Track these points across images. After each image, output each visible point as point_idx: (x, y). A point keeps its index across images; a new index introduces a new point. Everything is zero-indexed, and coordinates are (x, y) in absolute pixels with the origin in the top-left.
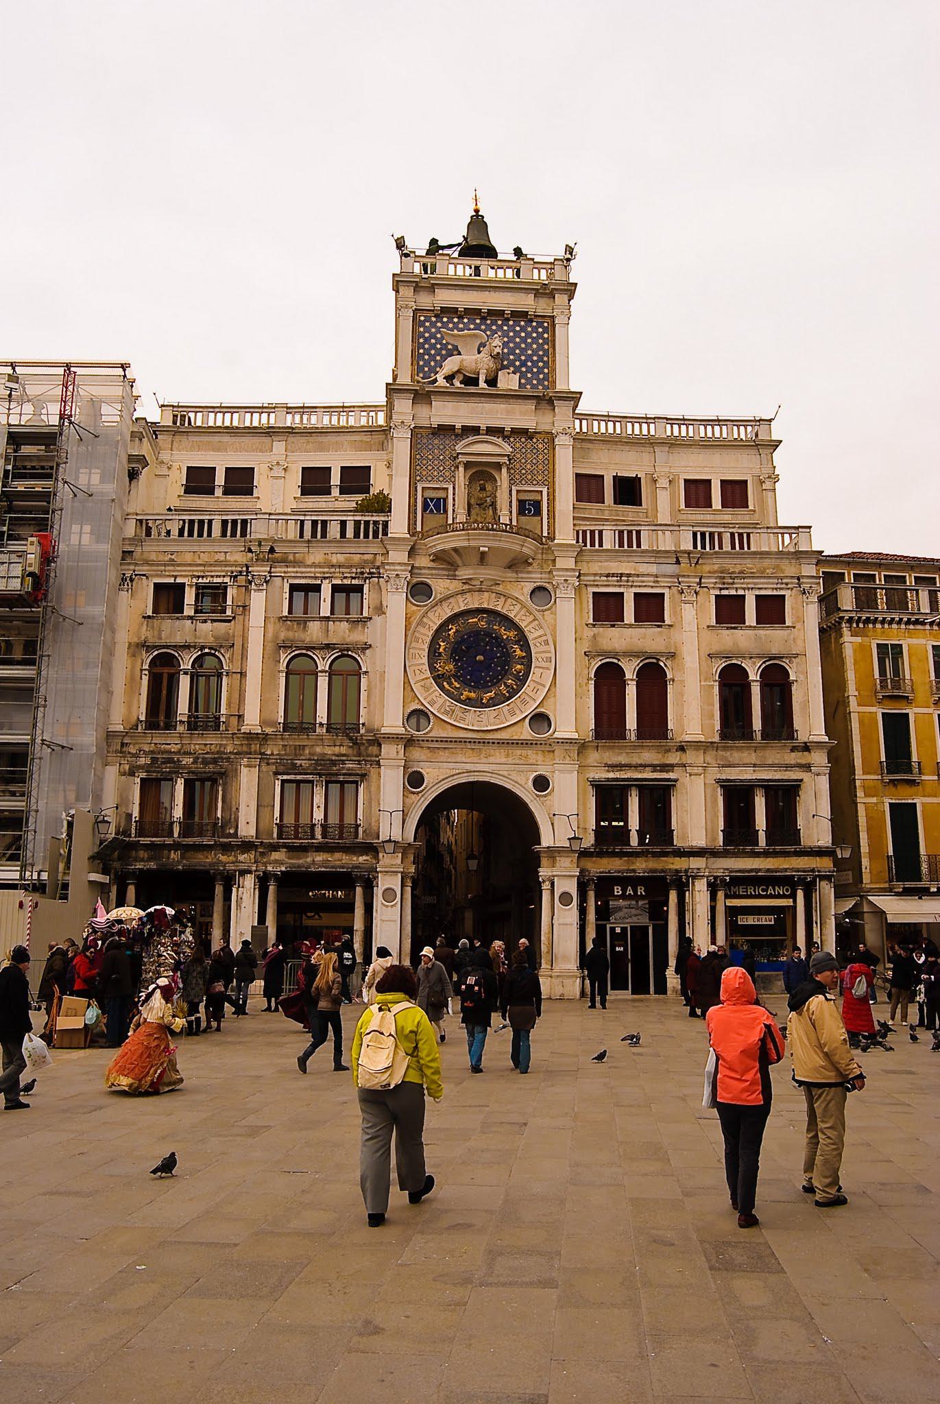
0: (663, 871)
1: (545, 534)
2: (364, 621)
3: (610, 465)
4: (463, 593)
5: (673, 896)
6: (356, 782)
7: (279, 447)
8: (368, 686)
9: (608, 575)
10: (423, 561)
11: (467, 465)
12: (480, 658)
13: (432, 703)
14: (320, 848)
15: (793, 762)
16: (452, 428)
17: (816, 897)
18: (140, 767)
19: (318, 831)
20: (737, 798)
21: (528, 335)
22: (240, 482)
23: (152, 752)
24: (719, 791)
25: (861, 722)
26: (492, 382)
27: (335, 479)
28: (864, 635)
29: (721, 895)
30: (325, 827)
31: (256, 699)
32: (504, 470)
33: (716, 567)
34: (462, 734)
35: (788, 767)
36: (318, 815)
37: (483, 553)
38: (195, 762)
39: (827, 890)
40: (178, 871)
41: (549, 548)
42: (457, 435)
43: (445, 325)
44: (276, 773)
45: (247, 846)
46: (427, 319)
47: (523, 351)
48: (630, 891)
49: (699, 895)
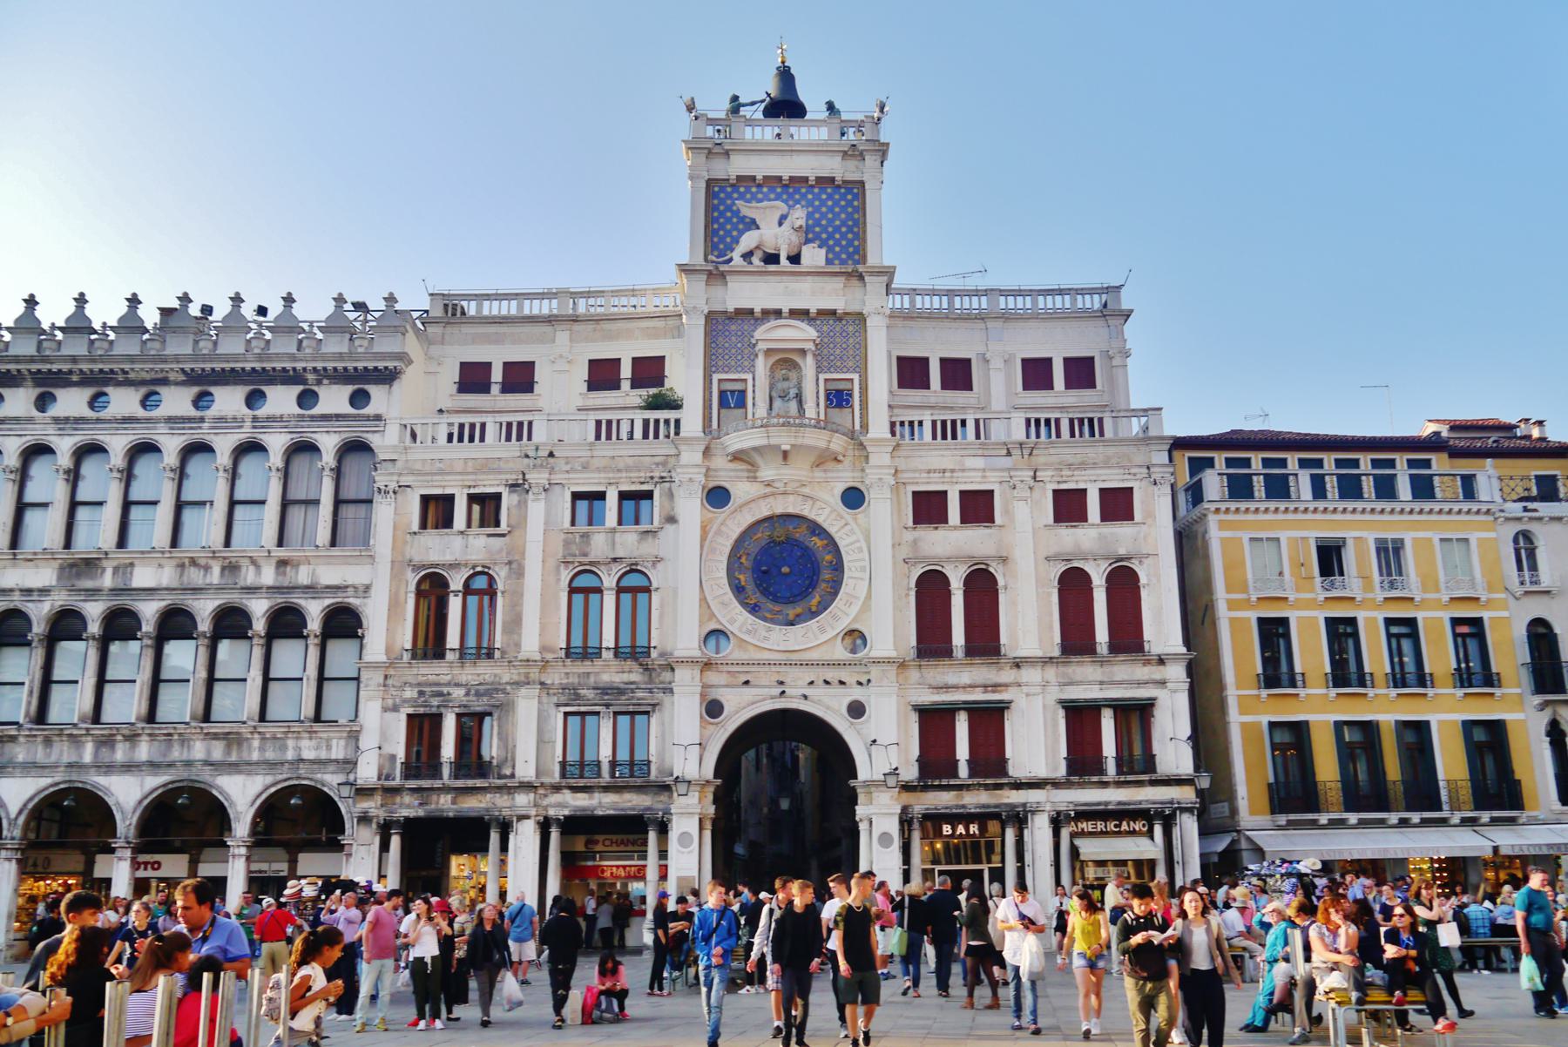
0: (996, 806)
1: (857, 427)
3: (935, 347)
4: (765, 496)
5: (1010, 834)
6: (647, 713)
7: (562, 335)
8: (662, 606)
9: (929, 472)
10: (719, 462)
11: (769, 352)
12: (785, 570)
13: (732, 621)
14: (606, 789)
15: (1146, 678)
16: (751, 312)
17: (1176, 832)
18: (405, 701)
20: (1081, 717)
23: (419, 684)
24: (1061, 713)
26: (795, 259)
27: (626, 371)
29: (1065, 833)
30: (614, 764)
31: (536, 618)
32: (810, 359)
33: (1054, 459)
34: (766, 655)
35: (1140, 684)
36: (605, 753)
37: (785, 454)
38: (467, 694)
39: (1188, 826)
40: (448, 819)
41: (861, 444)
42: (757, 319)
43: (742, 197)
44: (558, 705)
45: (527, 787)
47: (831, 221)
48: (961, 829)
49: (1039, 834)
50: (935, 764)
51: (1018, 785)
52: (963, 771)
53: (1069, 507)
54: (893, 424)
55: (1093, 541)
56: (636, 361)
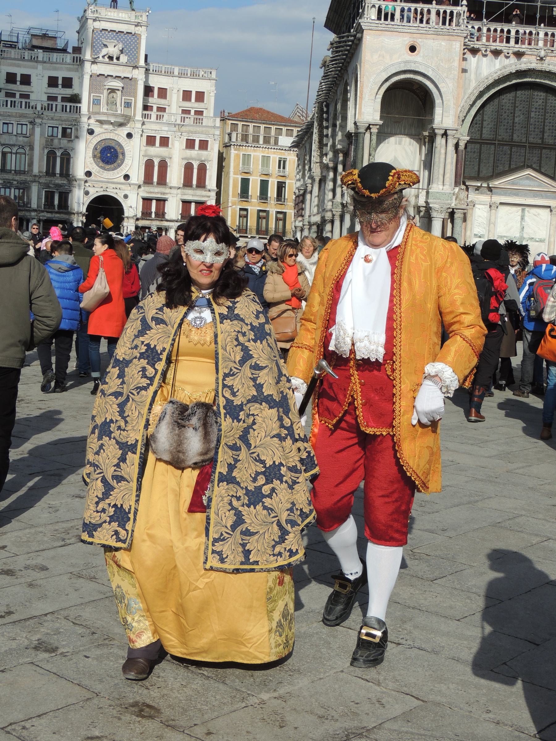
2: (72, 141)
7: (40, 67)
10: (92, 121)
11: (108, 89)
13: (93, 169)
14: (57, 213)
19: (56, 207)
21: (132, 41)
22: (26, 80)
25: (234, 180)
26: (118, 59)
27: (60, 82)
28: (238, 150)
35: (203, 196)
45: (35, 210)
46: (97, 32)
50: (146, 214)
51: (167, 221)
52: (153, 216)
53: (190, 144)
54: (143, 114)
55: (195, 153)
56: (63, 78)
